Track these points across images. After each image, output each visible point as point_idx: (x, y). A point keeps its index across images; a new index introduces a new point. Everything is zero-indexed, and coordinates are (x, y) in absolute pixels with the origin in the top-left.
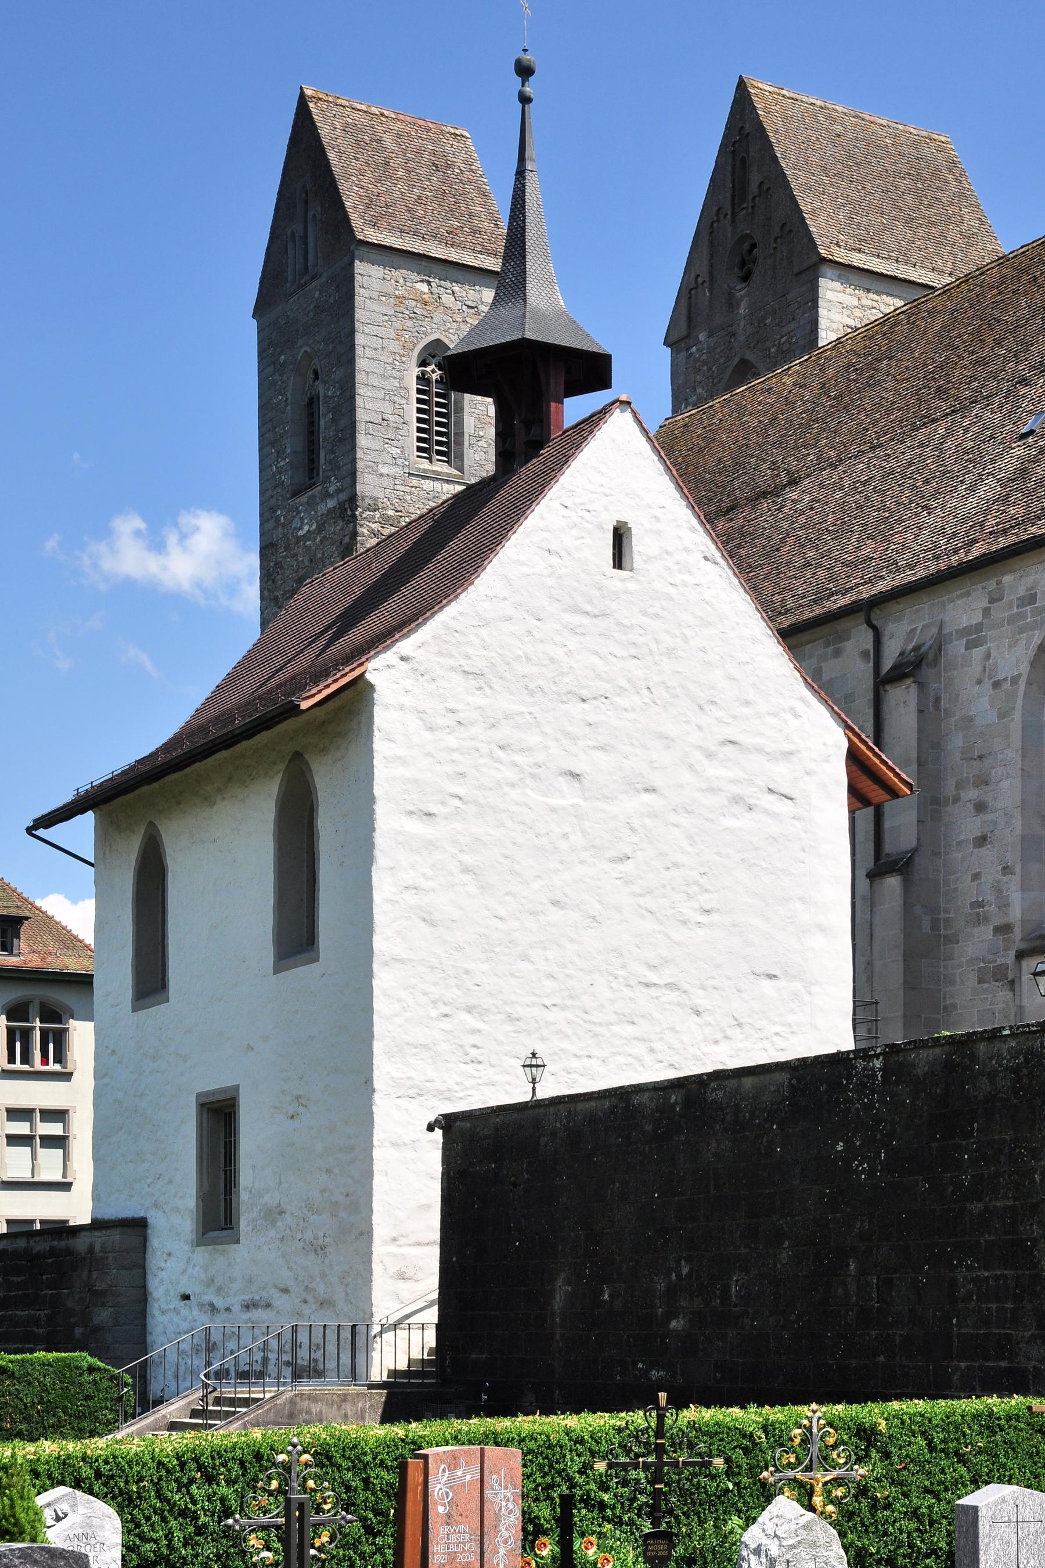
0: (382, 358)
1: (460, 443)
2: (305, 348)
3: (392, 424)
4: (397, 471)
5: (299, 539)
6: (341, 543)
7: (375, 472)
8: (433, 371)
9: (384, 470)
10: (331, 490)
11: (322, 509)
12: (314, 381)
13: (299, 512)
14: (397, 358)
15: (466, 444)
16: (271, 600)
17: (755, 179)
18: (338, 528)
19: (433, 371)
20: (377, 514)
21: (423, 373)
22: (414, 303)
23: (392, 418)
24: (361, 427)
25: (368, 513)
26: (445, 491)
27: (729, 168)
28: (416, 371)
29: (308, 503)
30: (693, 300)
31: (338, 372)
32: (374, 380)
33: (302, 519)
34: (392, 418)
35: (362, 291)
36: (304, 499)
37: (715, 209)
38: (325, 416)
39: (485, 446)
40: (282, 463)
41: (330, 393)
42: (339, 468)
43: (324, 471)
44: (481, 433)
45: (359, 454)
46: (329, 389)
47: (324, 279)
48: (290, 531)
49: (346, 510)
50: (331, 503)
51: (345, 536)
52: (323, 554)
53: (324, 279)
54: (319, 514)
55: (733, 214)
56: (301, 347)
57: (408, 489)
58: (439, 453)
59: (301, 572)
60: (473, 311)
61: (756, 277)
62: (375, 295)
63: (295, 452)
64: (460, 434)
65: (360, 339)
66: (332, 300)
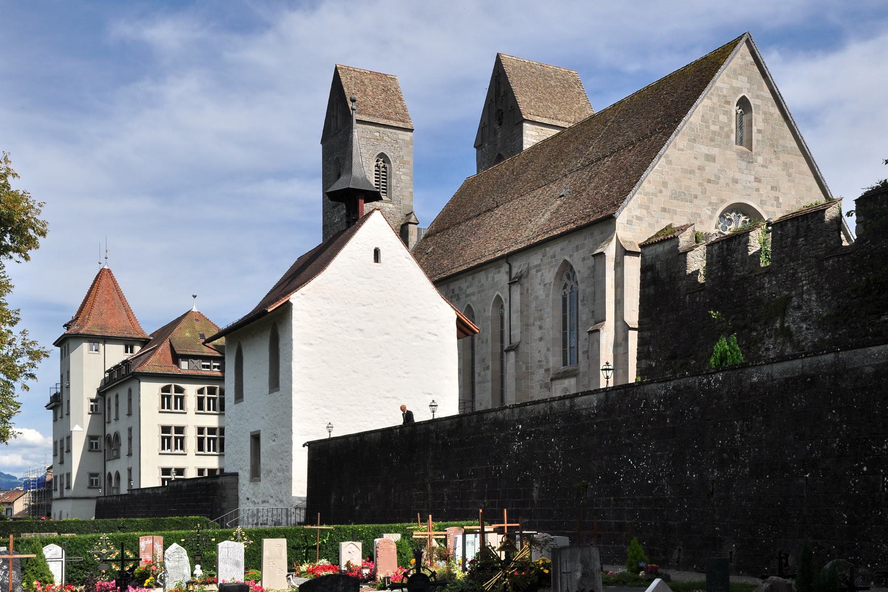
1: (390, 189)
2: (337, 156)
8: (381, 164)
13: (335, 214)
15: (393, 189)
17: (502, 90)
19: (381, 164)
21: (377, 164)
22: (373, 140)
28: (375, 163)
33: (336, 217)
36: (336, 209)
47: (342, 132)
55: (496, 102)
64: (391, 186)
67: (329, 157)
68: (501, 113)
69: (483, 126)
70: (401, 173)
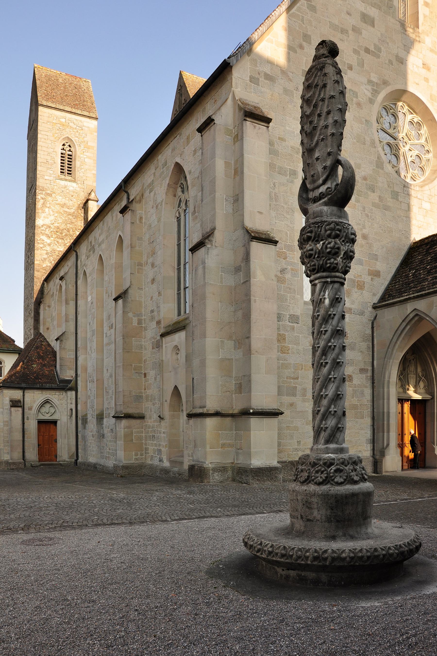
0: (47, 142)
1: (75, 170)
3: (50, 163)
4: (51, 178)
9: (46, 177)
14: (53, 142)
15: (77, 170)
20: (44, 192)
21: (63, 148)
22: (59, 125)
23: (50, 161)
24: (39, 164)
25: (41, 192)
26: (68, 185)
32: (44, 149)
34: (50, 161)
35: (41, 121)
39: (83, 171)
44: (82, 167)
45: (38, 172)
57: (55, 184)
58: (68, 173)
60: (80, 128)
62: (45, 122)
64: (75, 167)
65: (39, 136)
70: (85, 156)
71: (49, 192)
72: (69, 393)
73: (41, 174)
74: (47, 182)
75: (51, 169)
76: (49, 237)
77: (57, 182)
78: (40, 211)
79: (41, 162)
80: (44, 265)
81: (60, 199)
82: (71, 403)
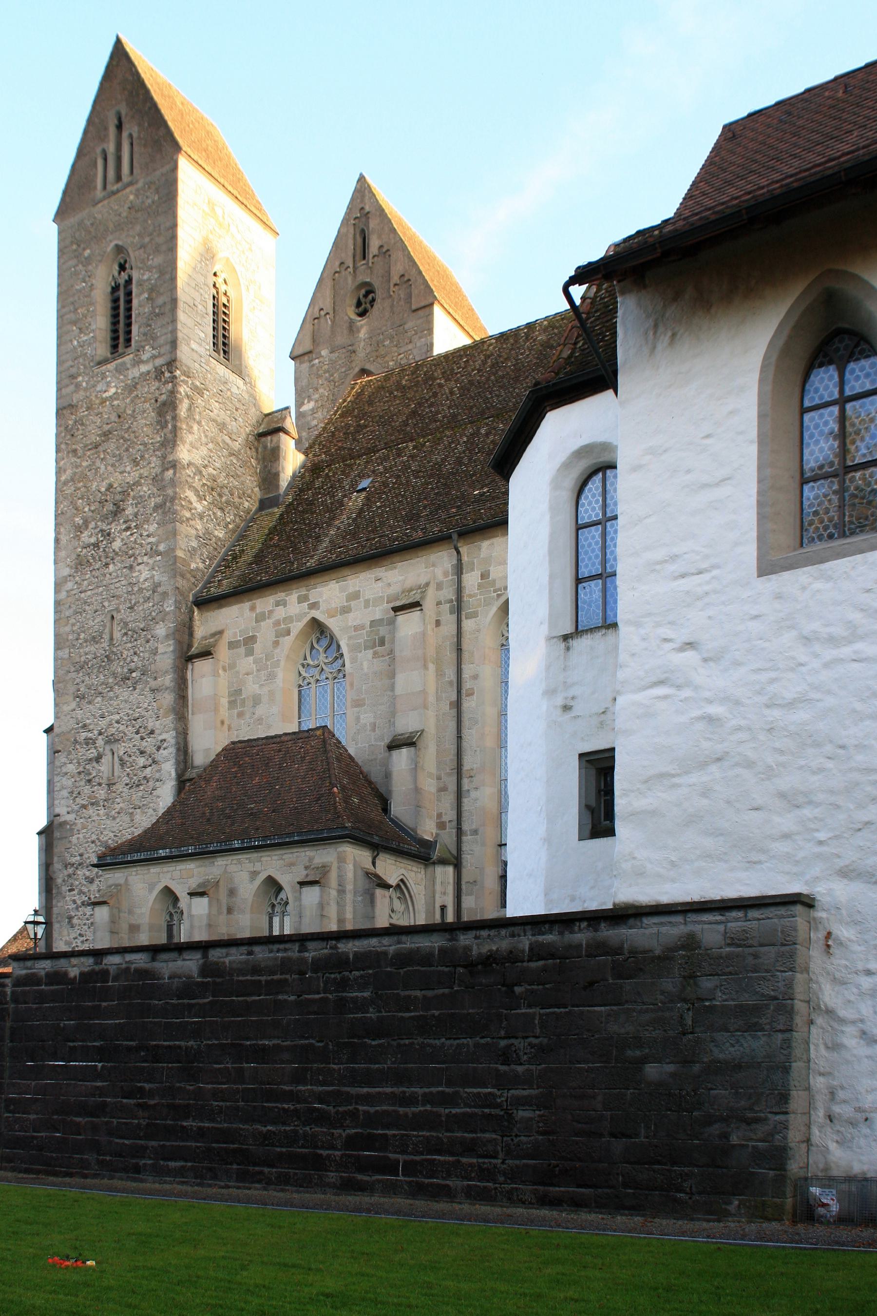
5: (103, 401)
6: (156, 401)
7: (188, 345)
9: (194, 346)
10: (144, 357)
11: (134, 373)
12: (120, 273)
16: (68, 452)
18: (154, 388)
27: (351, 236)
29: (116, 369)
30: (316, 326)
31: (155, 260)
33: (110, 382)
34: (200, 307)
36: (111, 366)
37: (337, 263)
38: (139, 295)
40: (85, 338)
41: (145, 277)
42: (154, 339)
43: (136, 342)
46: (143, 275)
47: (140, 184)
48: (94, 394)
49: (163, 373)
50: (144, 368)
51: (161, 394)
52: (134, 411)
53: (140, 184)
54: (130, 377)
55: (354, 267)
56: (111, 241)
57: (208, 368)
59: (106, 428)
61: (375, 311)
63: (100, 329)
66: (149, 201)
67: (84, 249)
68: (363, 292)
69: (317, 315)
71: (198, 384)
72: (439, 870)
73: (185, 332)
74: (196, 357)
75: (201, 328)
76: (201, 498)
77: (212, 365)
78: (184, 427)
79: (184, 302)
80: (193, 566)
81: (217, 411)
82: (445, 893)
